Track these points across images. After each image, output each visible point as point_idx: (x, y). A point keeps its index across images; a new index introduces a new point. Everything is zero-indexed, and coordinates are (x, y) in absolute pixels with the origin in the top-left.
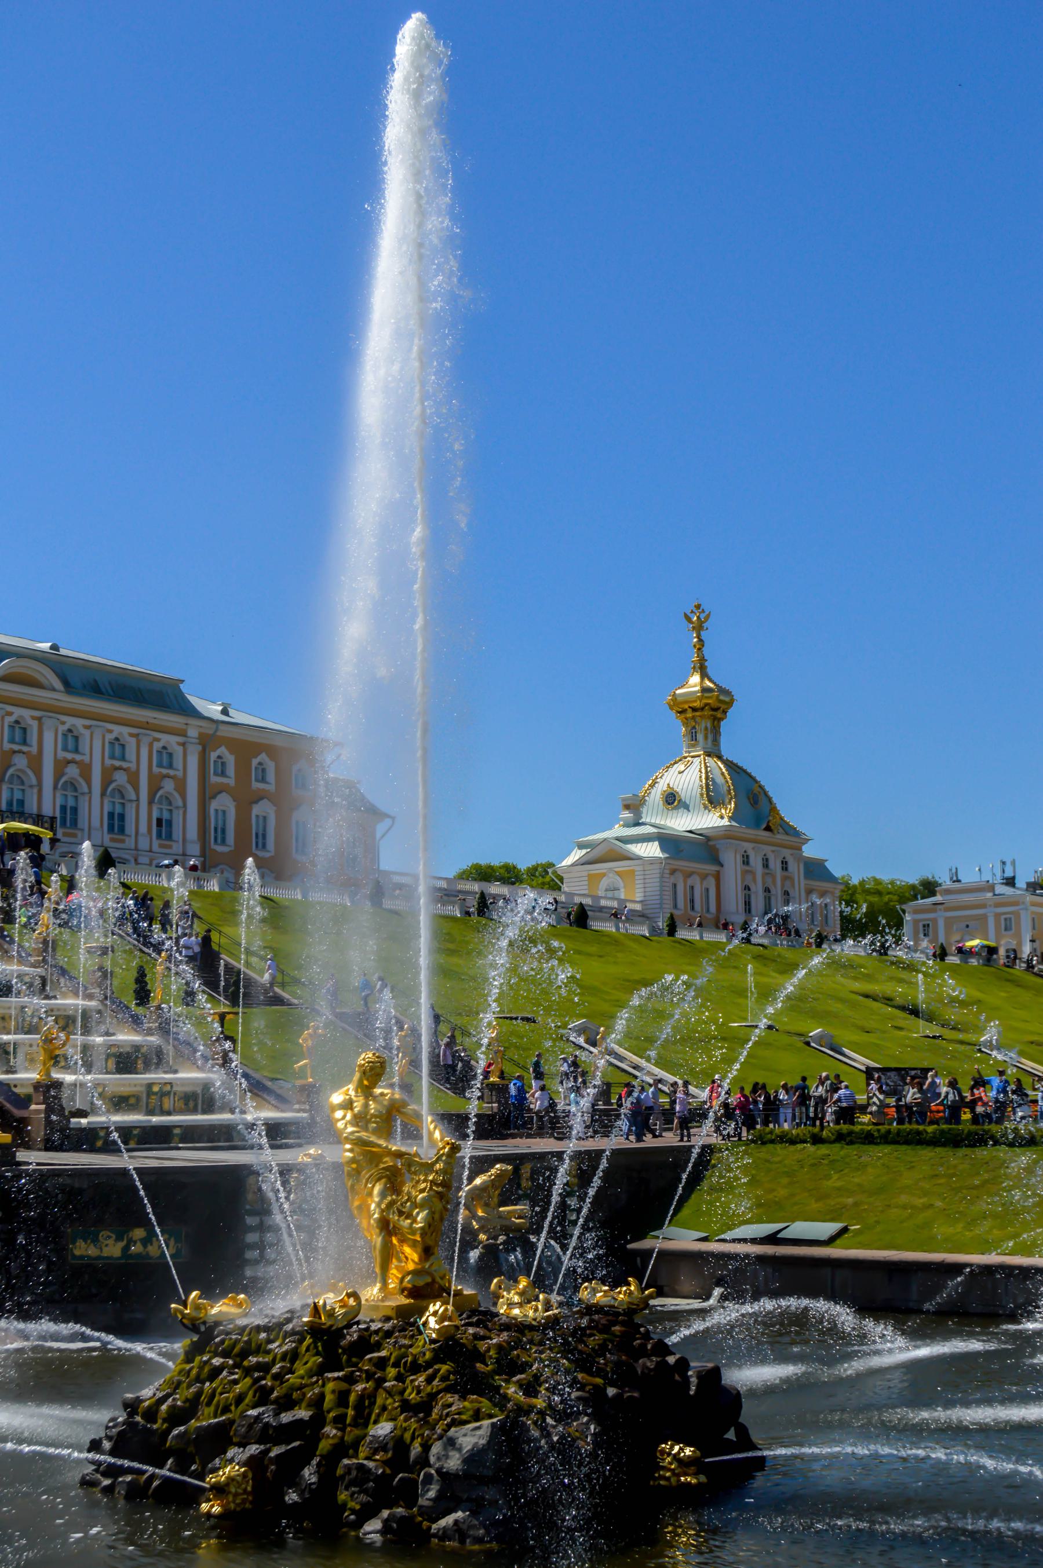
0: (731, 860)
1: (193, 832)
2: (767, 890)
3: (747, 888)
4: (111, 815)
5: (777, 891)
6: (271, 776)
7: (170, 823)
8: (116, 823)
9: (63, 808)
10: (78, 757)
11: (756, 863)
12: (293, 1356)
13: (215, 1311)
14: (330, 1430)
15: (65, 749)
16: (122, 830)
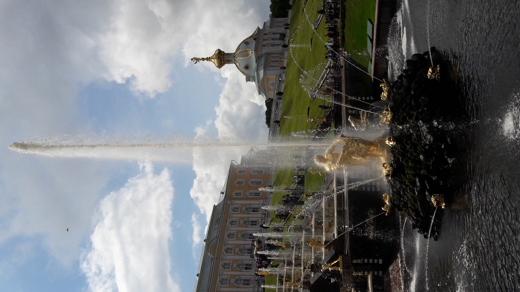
0: (265, 50)
1: (257, 202)
2: (273, 39)
3: (272, 45)
4: (252, 225)
5: (273, 36)
6: (241, 180)
7: (254, 208)
8: (254, 223)
9: (250, 238)
10: (236, 234)
11: (265, 43)
12: (401, 182)
13: (387, 203)
14: (422, 172)
15: (233, 238)
16: (256, 222)
